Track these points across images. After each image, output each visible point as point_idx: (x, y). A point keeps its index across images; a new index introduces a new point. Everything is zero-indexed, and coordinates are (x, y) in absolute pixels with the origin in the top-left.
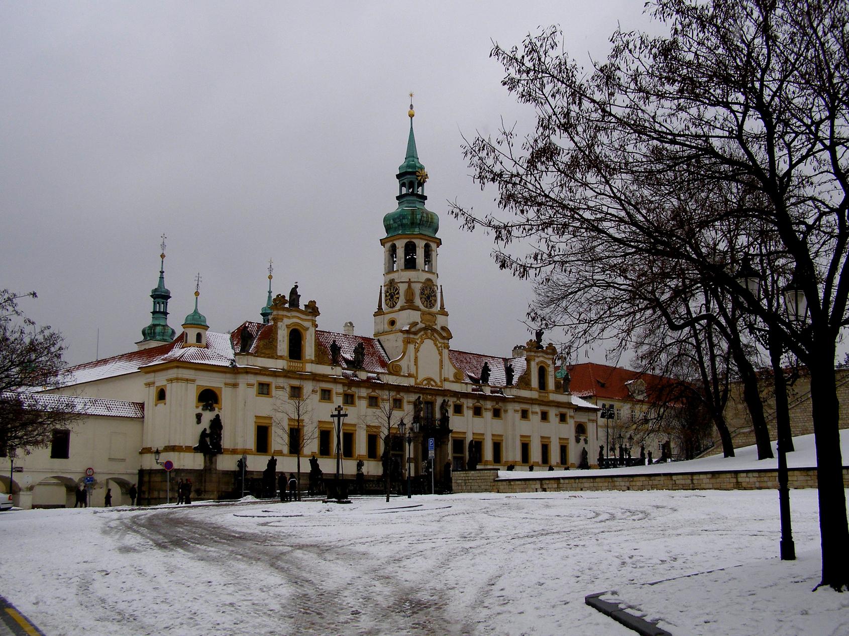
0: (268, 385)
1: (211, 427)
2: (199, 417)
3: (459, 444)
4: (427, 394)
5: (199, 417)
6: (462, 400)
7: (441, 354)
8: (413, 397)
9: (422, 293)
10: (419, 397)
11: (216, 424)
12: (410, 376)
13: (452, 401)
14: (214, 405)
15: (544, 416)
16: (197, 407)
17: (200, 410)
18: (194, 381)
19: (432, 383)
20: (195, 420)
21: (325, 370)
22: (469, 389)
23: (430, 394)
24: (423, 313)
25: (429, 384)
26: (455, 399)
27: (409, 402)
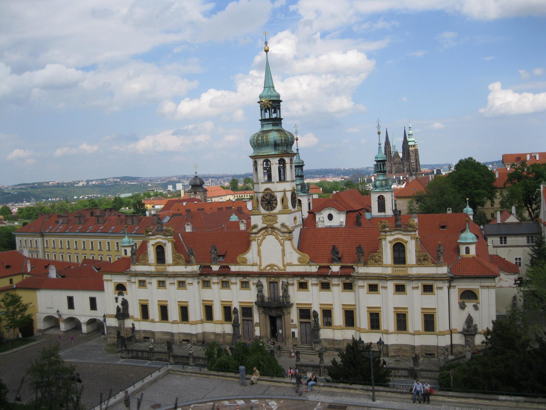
0: (144, 281)
1: (122, 304)
2: (117, 299)
3: (305, 313)
4: (270, 277)
5: (117, 299)
6: (306, 279)
7: (282, 245)
8: (255, 280)
9: (262, 200)
10: (259, 281)
11: (125, 303)
12: (253, 265)
13: (295, 281)
14: (124, 292)
15: (400, 289)
16: (115, 294)
17: (116, 296)
18: (112, 280)
19: (275, 268)
20: (114, 300)
21: (181, 269)
22: (314, 269)
23: (273, 277)
24: (264, 216)
25: (272, 268)
26: (299, 279)
27: (254, 284)
